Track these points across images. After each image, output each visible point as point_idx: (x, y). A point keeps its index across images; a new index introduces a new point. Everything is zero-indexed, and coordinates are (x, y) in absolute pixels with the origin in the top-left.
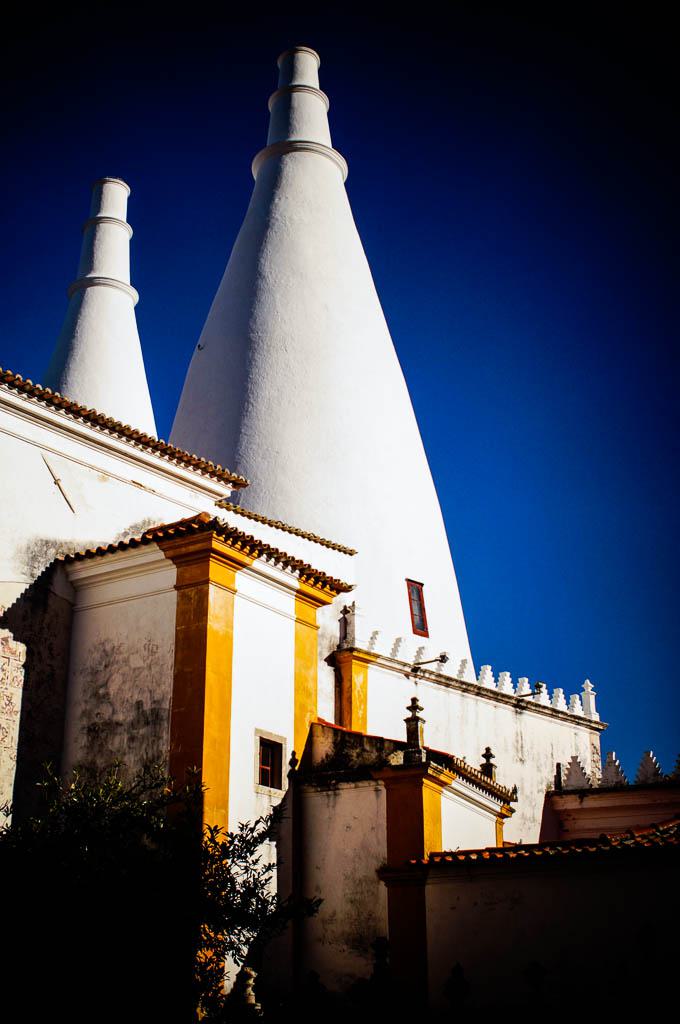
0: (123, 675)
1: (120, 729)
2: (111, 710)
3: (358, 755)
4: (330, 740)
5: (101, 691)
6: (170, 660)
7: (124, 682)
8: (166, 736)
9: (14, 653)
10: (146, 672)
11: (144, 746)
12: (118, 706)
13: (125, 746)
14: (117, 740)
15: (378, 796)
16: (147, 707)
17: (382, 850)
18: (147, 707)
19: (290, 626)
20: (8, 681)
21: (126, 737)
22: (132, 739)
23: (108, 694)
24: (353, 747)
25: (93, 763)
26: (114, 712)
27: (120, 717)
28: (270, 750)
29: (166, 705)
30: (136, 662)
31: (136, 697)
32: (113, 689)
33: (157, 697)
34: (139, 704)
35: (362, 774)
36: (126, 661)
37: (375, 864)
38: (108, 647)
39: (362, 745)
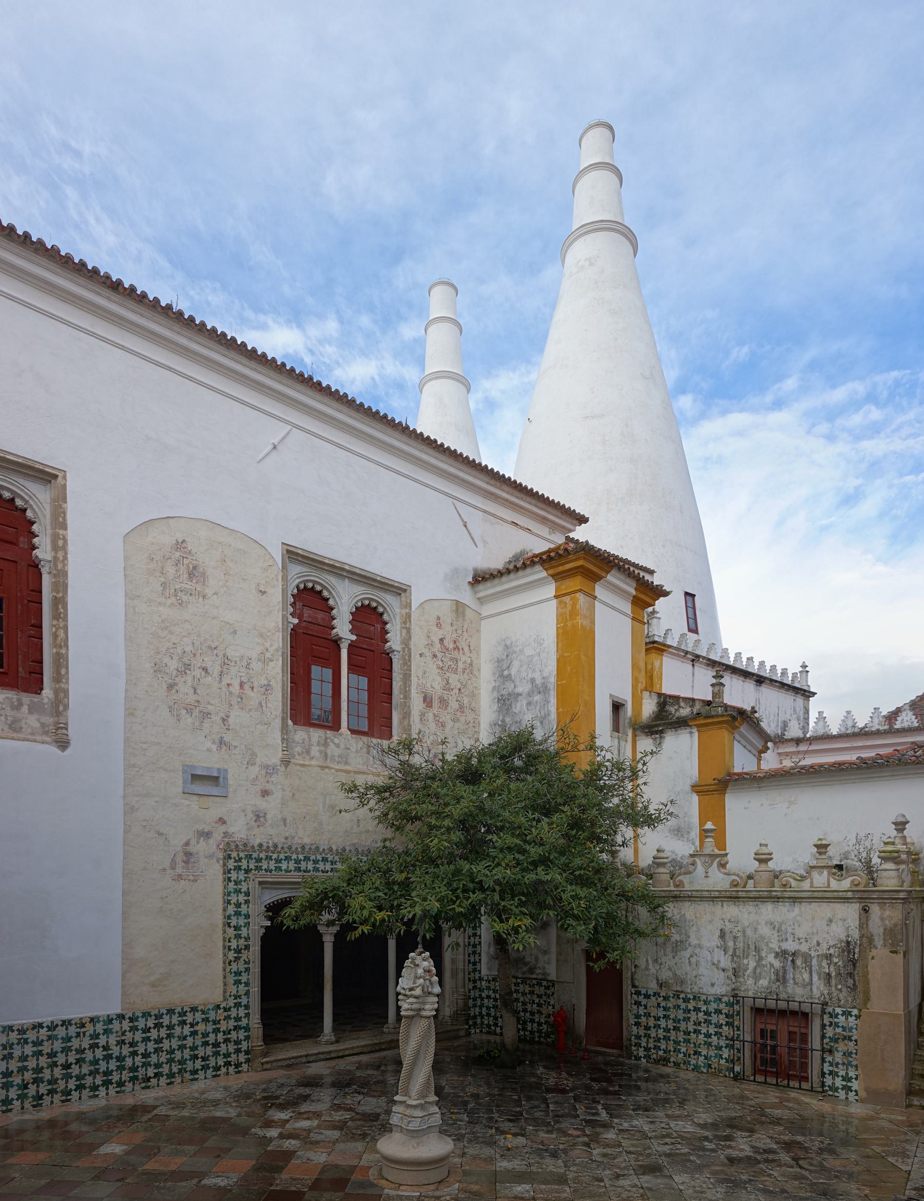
0: (520, 661)
1: (520, 698)
2: (513, 685)
3: (676, 710)
4: (656, 701)
5: (506, 673)
6: (553, 648)
7: (521, 666)
8: (553, 700)
9: (447, 649)
10: (536, 658)
11: (538, 708)
12: (517, 683)
13: (525, 708)
14: (519, 704)
15: (691, 737)
16: (539, 681)
17: (695, 772)
18: (539, 681)
19: (626, 624)
20: (446, 668)
21: (525, 702)
22: (529, 704)
23: (510, 675)
24: (672, 705)
25: (503, 721)
26: (515, 687)
27: (520, 690)
28: (617, 707)
29: (553, 680)
30: (529, 652)
31: (530, 675)
32: (513, 671)
33: (545, 675)
34: (533, 680)
35: (681, 723)
36: (522, 651)
37: (689, 782)
38: (508, 643)
39: (678, 704)
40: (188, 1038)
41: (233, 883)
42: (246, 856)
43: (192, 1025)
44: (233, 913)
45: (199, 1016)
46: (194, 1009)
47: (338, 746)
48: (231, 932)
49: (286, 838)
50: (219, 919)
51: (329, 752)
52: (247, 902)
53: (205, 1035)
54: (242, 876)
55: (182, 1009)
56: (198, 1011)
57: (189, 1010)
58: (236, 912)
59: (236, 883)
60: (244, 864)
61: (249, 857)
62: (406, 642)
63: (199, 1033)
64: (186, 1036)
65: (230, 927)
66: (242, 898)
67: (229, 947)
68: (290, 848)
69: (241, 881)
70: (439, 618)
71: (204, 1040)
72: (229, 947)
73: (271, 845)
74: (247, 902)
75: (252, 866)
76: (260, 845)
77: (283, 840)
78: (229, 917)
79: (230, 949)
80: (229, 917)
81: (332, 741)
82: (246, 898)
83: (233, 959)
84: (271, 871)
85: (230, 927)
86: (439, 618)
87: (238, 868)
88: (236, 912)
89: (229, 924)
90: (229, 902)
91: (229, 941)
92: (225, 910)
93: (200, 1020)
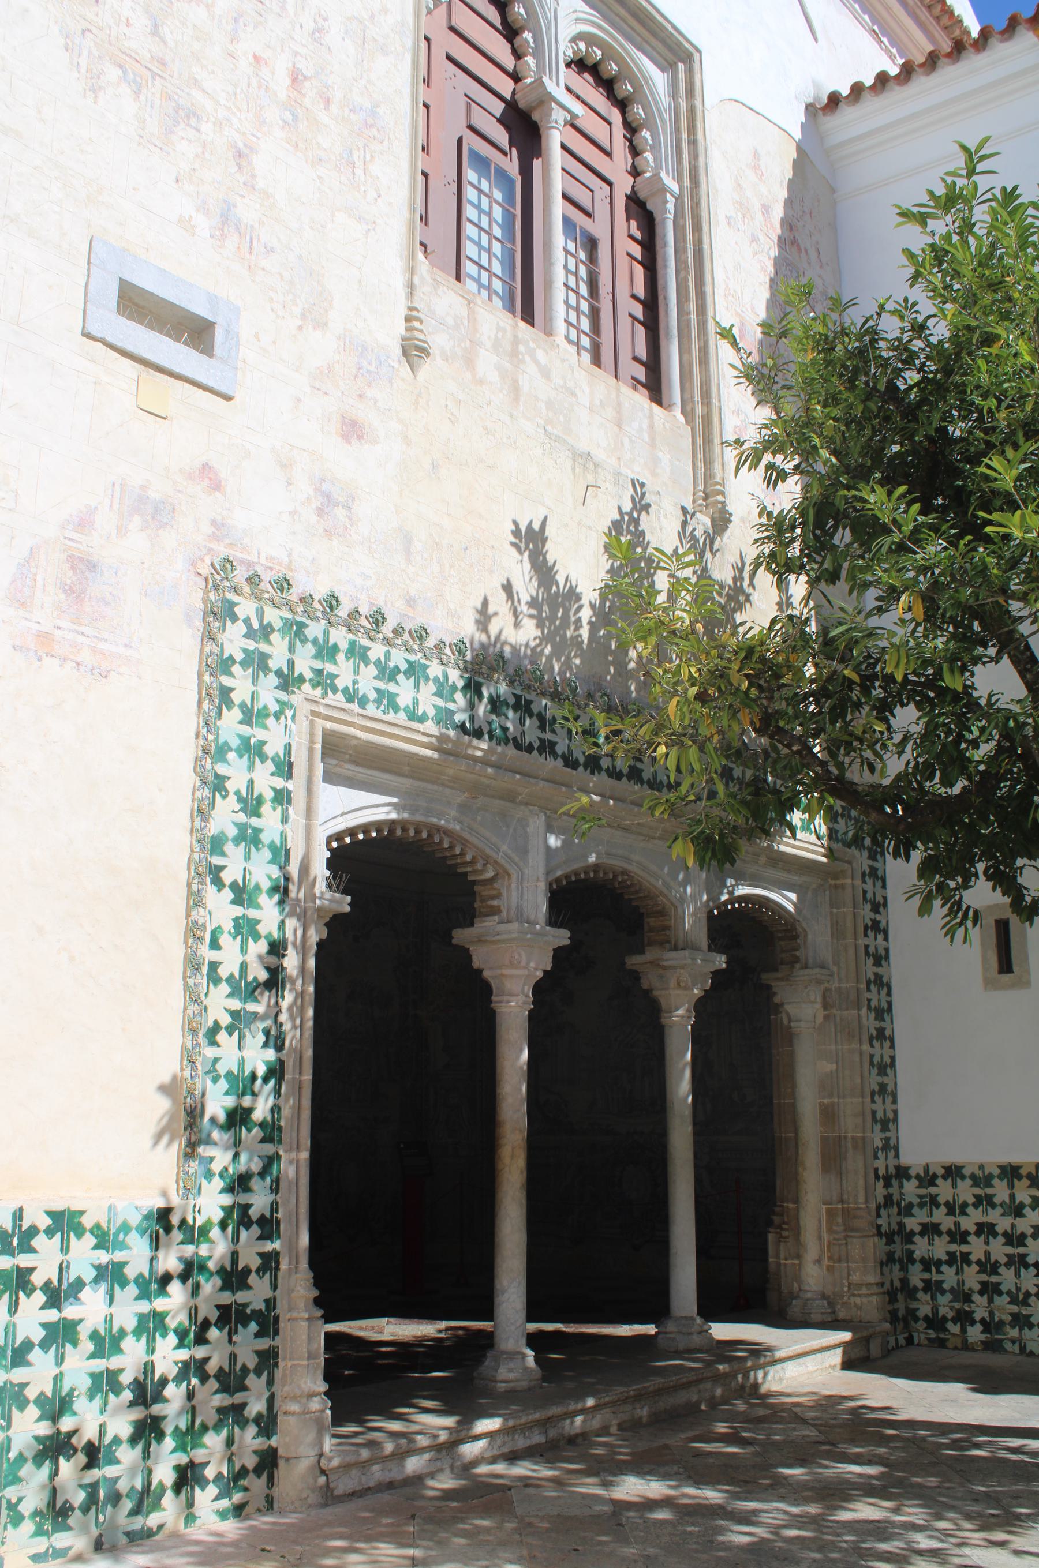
40: (36, 1355)
41: (236, 714)
42: (288, 624)
43: (55, 1297)
44: (232, 832)
45: (84, 1257)
46: (65, 1223)
47: (546, 373)
48: (220, 908)
49: (411, 602)
50: (176, 847)
51: (524, 381)
52: (282, 797)
53: (107, 1343)
54: (268, 694)
55: (18, 1215)
56: (80, 1231)
57: (44, 1222)
58: (242, 828)
59: (251, 715)
60: (278, 651)
61: (296, 631)
62: (694, 178)
63: (84, 1332)
64: (28, 1345)
65: (218, 882)
66: (266, 780)
67: (214, 966)
68: (421, 634)
69: (264, 713)
70: (756, 155)
71: (99, 1365)
72: (214, 966)
73: (364, 610)
74: (282, 797)
75: (305, 664)
76: (332, 602)
77: (400, 604)
78: (217, 845)
79: (214, 978)
80: (217, 845)
81: (532, 353)
82: (279, 783)
83: (225, 1020)
84: (363, 702)
85: (218, 882)
86: (756, 155)
87: (258, 663)
88: (242, 828)
89: (216, 873)
90: (219, 785)
91: (215, 945)
92: (203, 812)
93: (89, 1275)
